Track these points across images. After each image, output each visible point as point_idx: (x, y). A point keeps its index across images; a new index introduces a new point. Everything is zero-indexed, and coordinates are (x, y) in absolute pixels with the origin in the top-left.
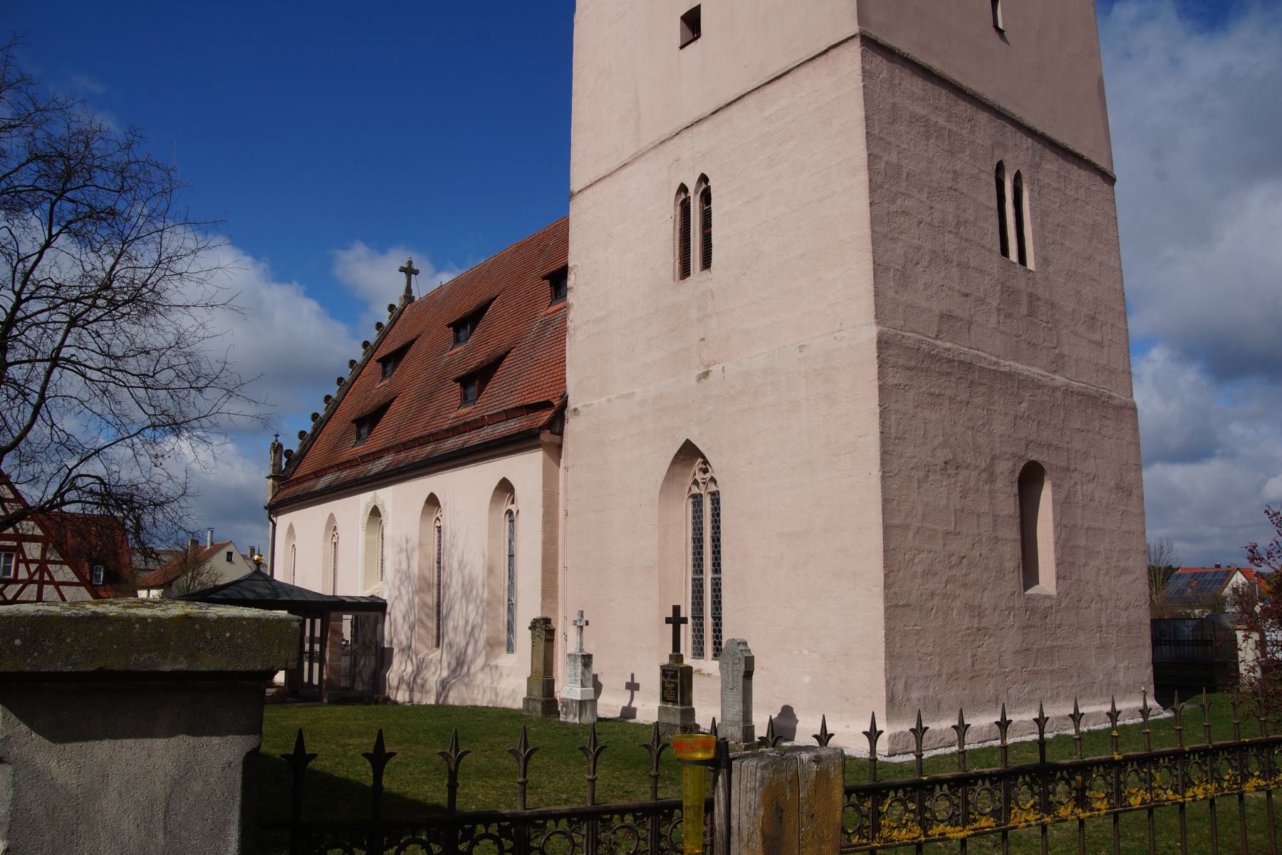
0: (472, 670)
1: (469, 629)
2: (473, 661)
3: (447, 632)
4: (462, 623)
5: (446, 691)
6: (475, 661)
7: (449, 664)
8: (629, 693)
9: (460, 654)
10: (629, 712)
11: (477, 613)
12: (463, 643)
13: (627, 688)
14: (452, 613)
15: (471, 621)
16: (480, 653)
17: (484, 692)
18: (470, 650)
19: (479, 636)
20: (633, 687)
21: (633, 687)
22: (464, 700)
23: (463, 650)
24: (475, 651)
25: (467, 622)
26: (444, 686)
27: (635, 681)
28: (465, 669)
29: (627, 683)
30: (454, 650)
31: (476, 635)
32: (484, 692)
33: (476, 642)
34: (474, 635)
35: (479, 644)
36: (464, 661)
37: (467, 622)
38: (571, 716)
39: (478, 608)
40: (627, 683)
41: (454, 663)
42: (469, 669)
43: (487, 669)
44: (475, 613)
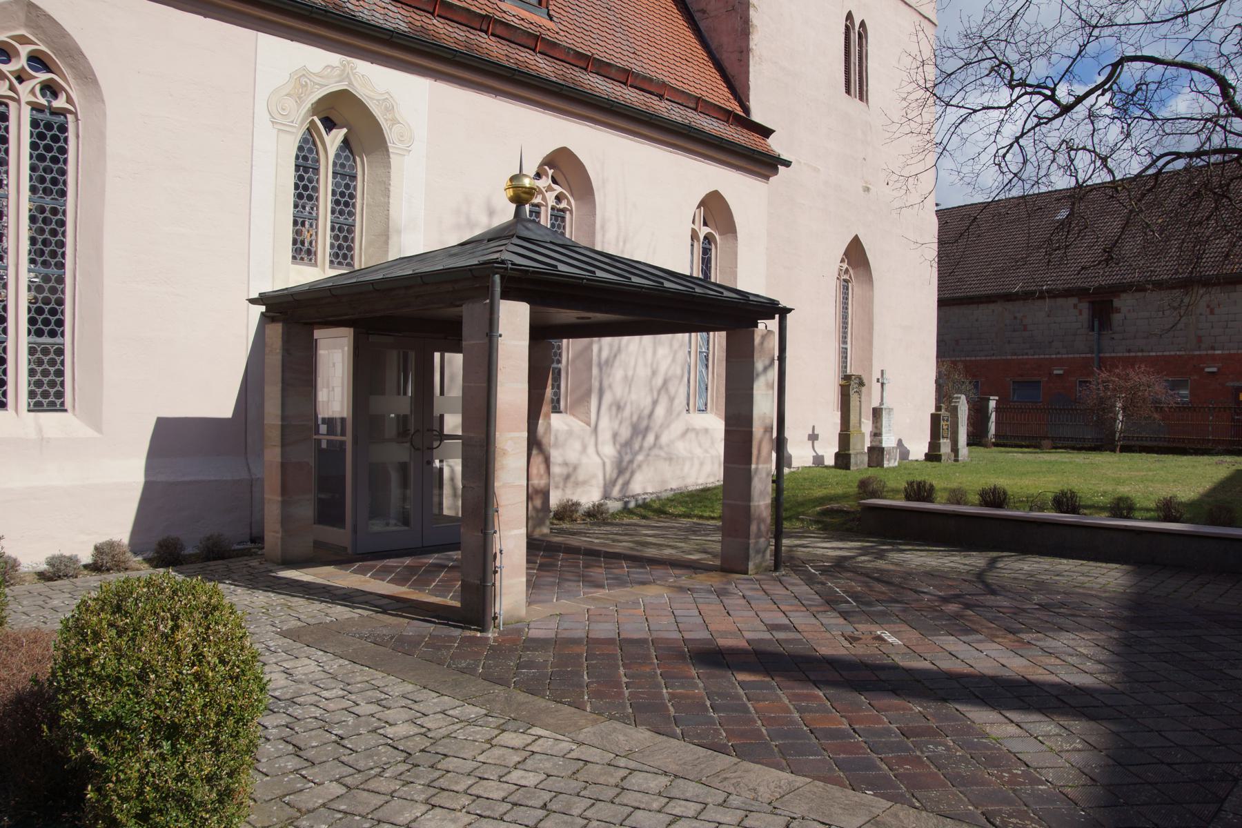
0: (664, 439)
1: (659, 381)
2: (665, 425)
3: (610, 386)
4: (643, 372)
5: (627, 475)
6: (668, 426)
7: (615, 436)
8: (811, 442)
9: (640, 418)
10: (818, 460)
11: (674, 360)
12: (646, 402)
13: (809, 439)
14: (623, 356)
15: (663, 368)
16: (679, 414)
17: (702, 464)
18: (660, 411)
19: (677, 392)
20: (813, 437)
21: (813, 437)
22: (664, 482)
23: (647, 412)
24: (669, 410)
25: (654, 373)
26: (623, 468)
27: (816, 433)
28: (650, 438)
29: (809, 435)
30: (627, 413)
31: (672, 390)
32: (702, 464)
33: (672, 400)
34: (667, 390)
35: (677, 402)
36: (647, 429)
37: (654, 373)
38: (893, 461)
39: (675, 353)
40: (809, 435)
41: (625, 433)
42: (657, 437)
43: (691, 435)
44: (669, 360)
